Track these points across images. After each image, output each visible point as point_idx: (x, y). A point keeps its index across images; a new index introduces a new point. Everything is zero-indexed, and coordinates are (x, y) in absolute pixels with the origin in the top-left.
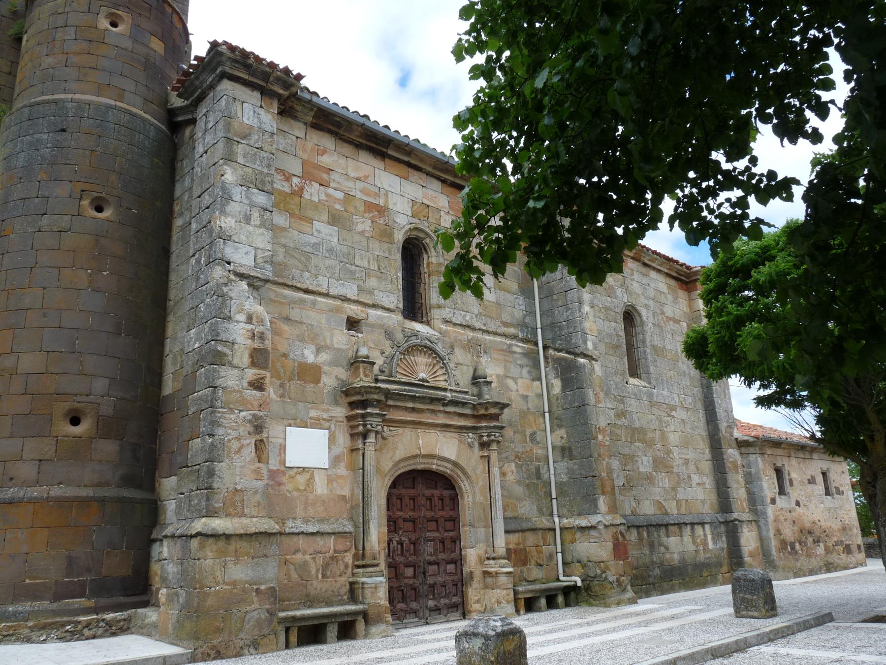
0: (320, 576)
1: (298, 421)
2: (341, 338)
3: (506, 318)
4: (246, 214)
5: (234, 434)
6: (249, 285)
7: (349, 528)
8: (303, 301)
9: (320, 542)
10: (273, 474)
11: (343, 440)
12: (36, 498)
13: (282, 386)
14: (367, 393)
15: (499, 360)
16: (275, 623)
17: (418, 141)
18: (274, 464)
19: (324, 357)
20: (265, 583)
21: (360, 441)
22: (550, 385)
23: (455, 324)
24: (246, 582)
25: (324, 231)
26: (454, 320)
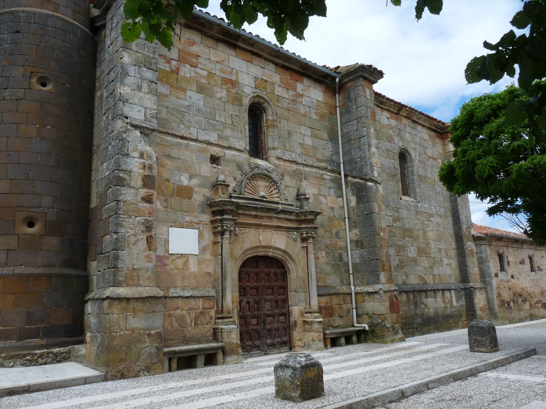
0: (193, 324)
2: (206, 169)
3: (320, 156)
4: (138, 85)
5: (132, 232)
6: (141, 133)
7: (213, 293)
9: (193, 302)
10: (159, 259)
11: (208, 236)
12: (5, 274)
13: (166, 200)
14: (224, 205)
15: (314, 184)
16: (161, 355)
17: (258, 36)
18: (160, 252)
19: (194, 182)
20: (155, 329)
21: (219, 237)
22: (349, 200)
23: (285, 160)
24: (141, 329)
25: (194, 97)
26: (284, 158)
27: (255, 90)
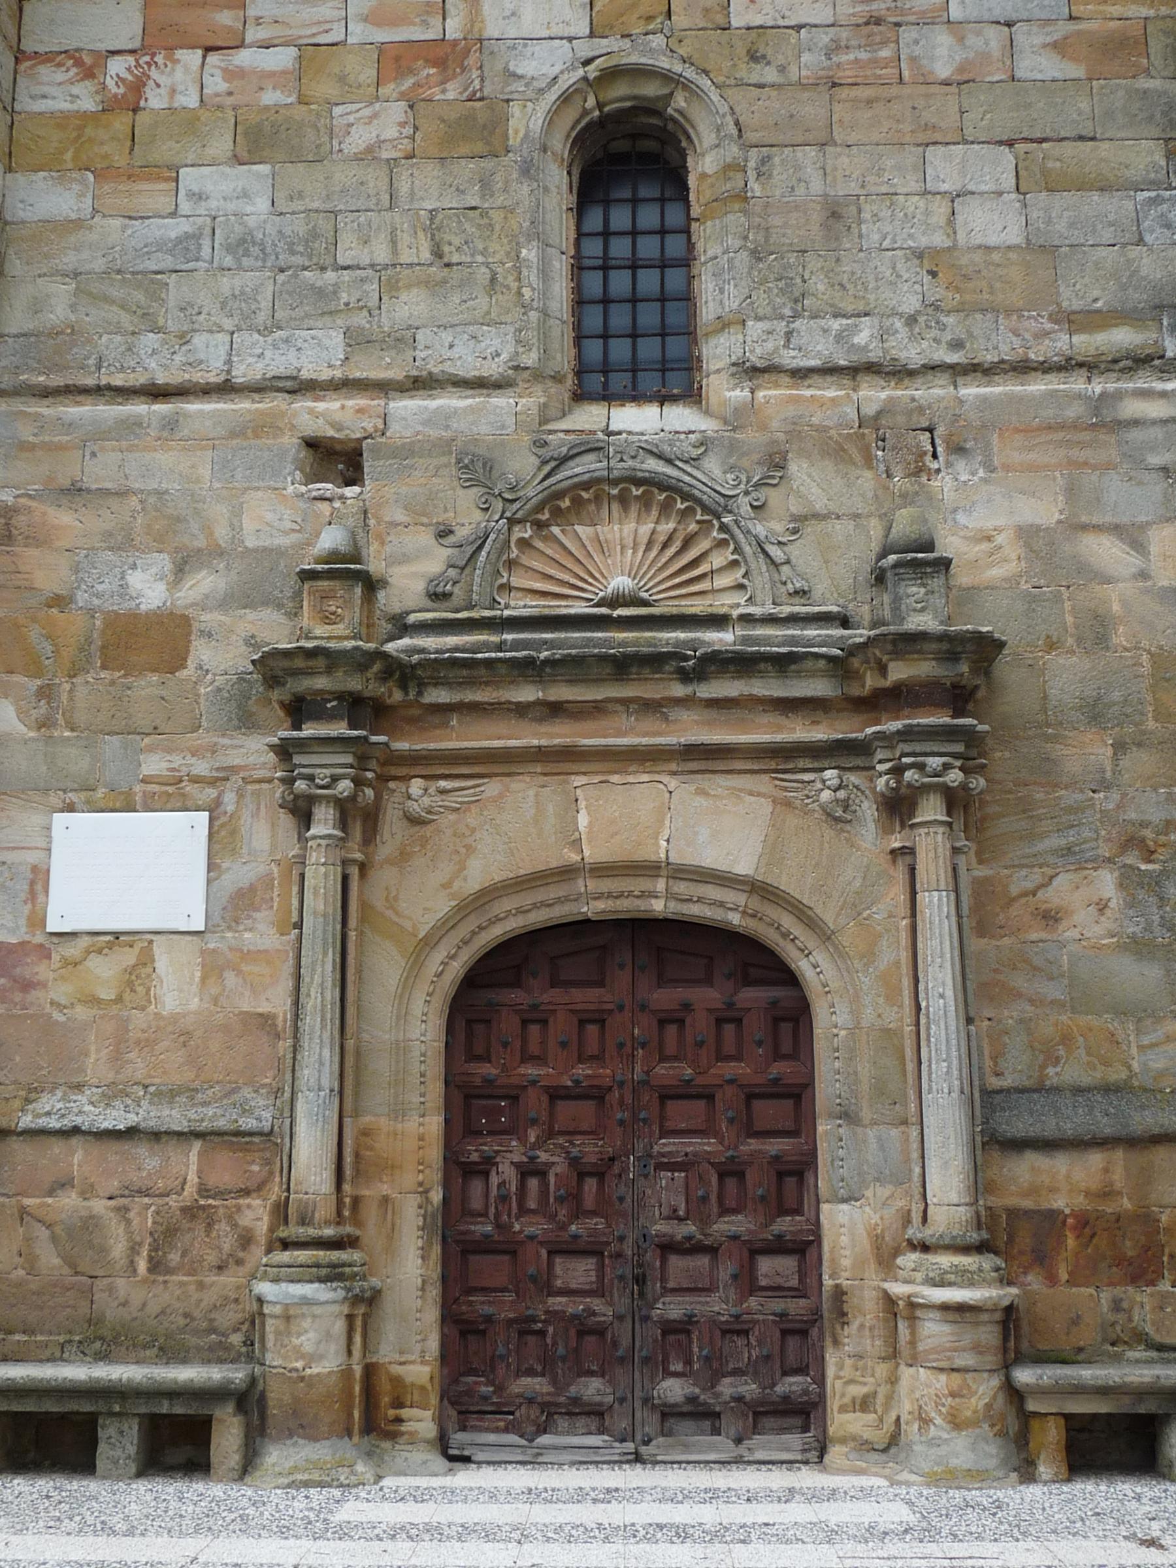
0: (142, 1266)
1: (100, 792)
2: (284, 517)
3: (1083, 290)
8: (133, 426)
9: (147, 1161)
13: (46, 693)
15: (1033, 468)
19: (204, 583)
23: (800, 374)
25: (225, 190)
26: (790, 358)
27: (585, 49)
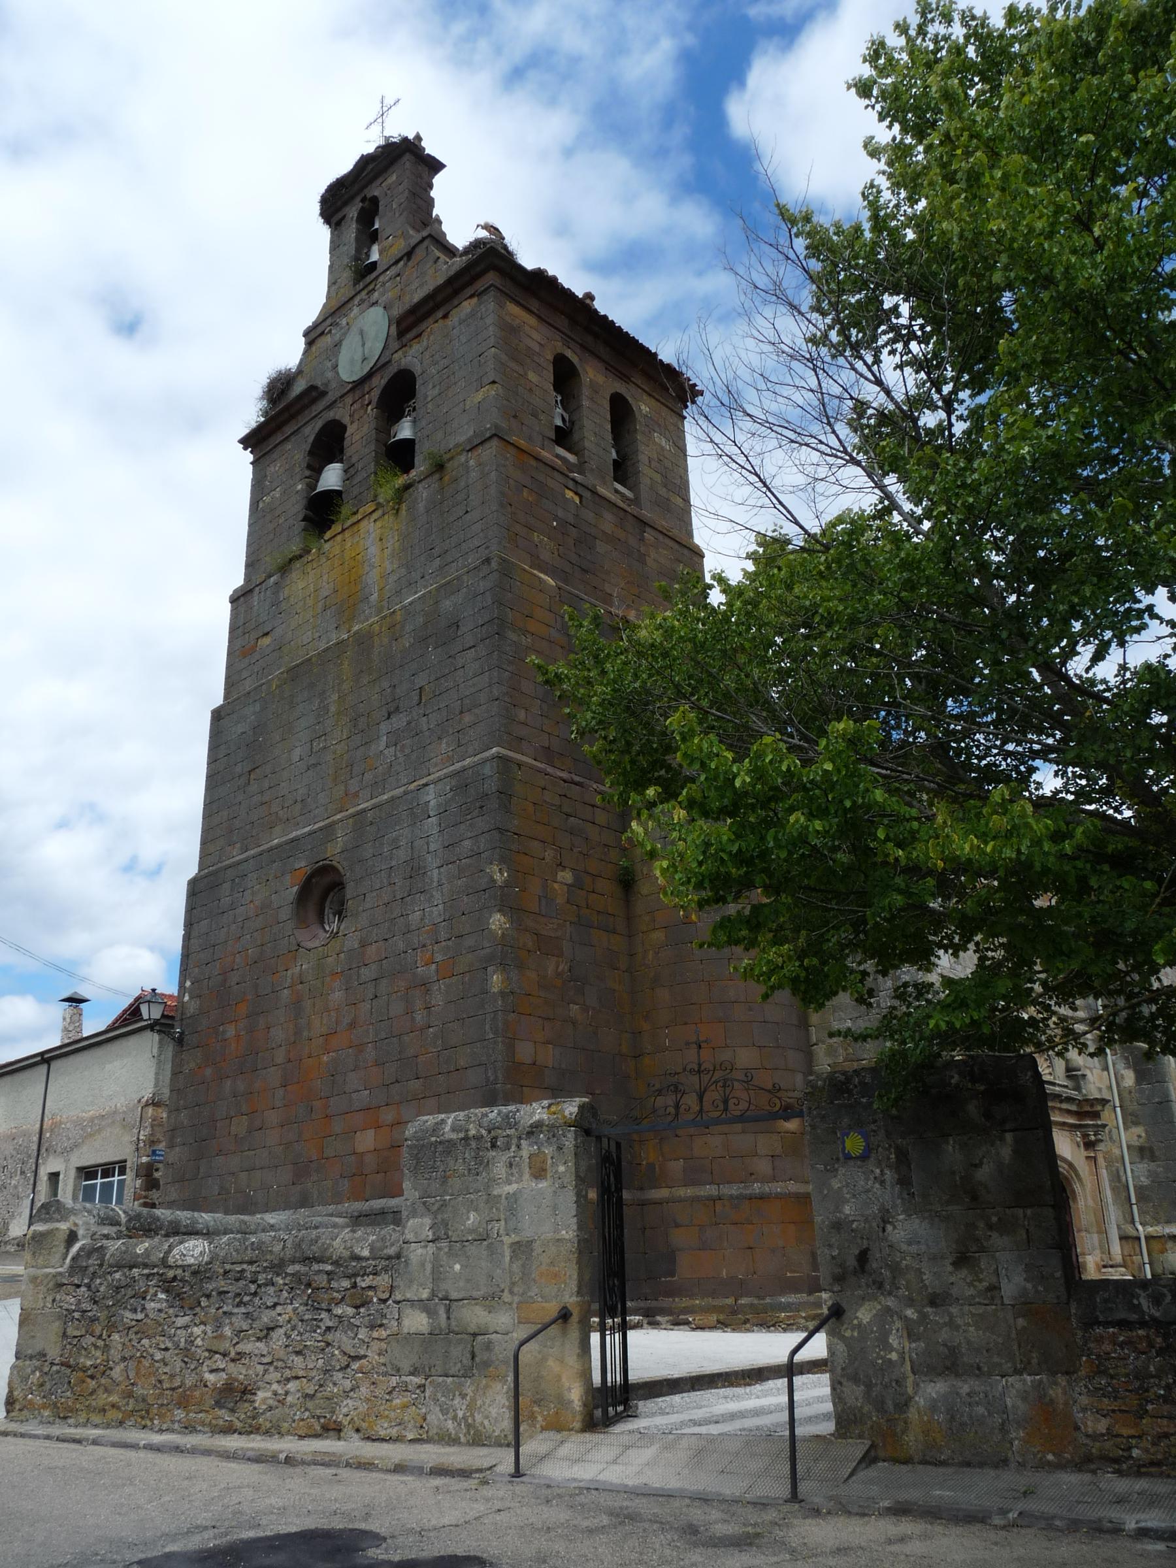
22: (1119, 1076)
